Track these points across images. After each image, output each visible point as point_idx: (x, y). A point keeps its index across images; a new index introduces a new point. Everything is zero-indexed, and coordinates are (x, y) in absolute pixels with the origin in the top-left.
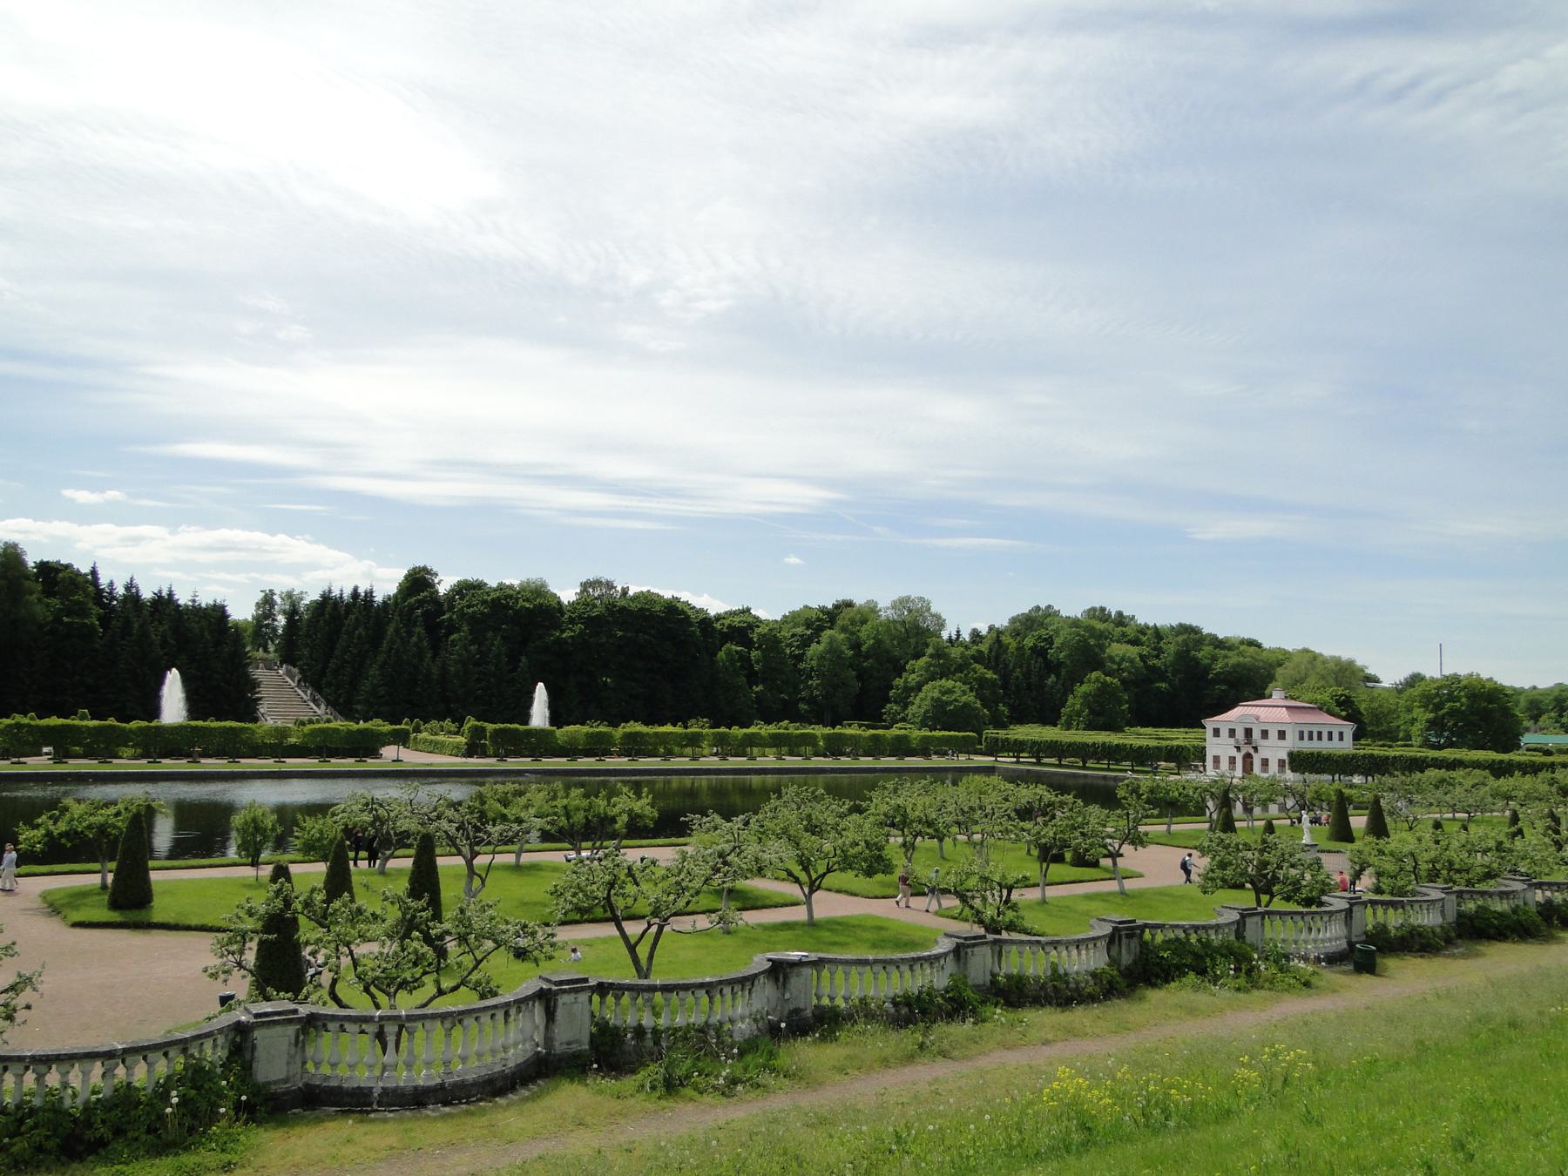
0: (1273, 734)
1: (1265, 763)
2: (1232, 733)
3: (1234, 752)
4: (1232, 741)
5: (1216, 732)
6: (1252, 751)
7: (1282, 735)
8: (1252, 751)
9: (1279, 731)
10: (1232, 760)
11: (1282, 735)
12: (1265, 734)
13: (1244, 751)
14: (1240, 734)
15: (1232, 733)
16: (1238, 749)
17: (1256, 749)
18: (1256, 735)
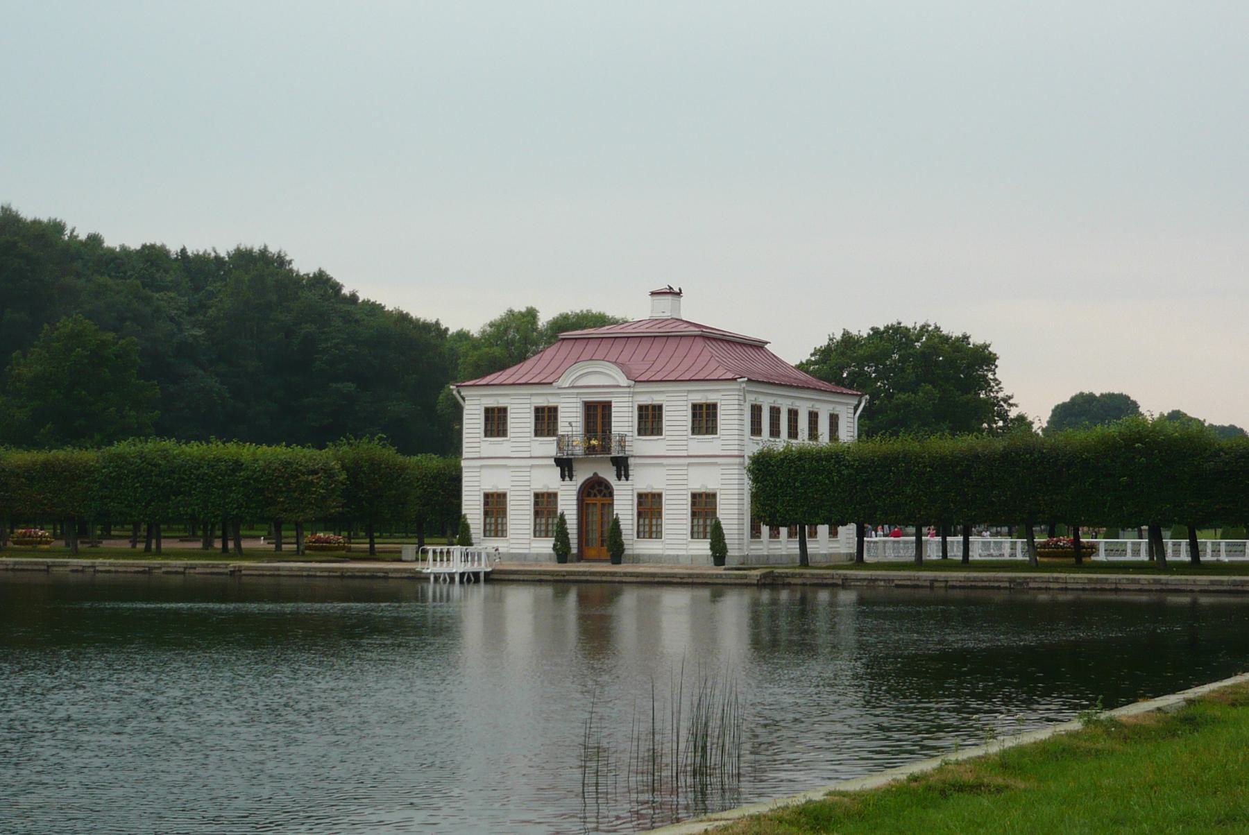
0: (677, 414)
1: (649, 506)
2: (546, 420)
3: (549, 479)
4: (548, 447)
5: (496, 422)
6: (609, 475)
7: (704, 418)
8: (609, 475)
9: (696, 408)
10: (544, 503)
11: (704, 418)
12: (650, 420)
13: (581, 476)
14: (571, 420)
15: (546, 420)
16: (565, 466)
17: (622, 466)
18: (623, 421)
